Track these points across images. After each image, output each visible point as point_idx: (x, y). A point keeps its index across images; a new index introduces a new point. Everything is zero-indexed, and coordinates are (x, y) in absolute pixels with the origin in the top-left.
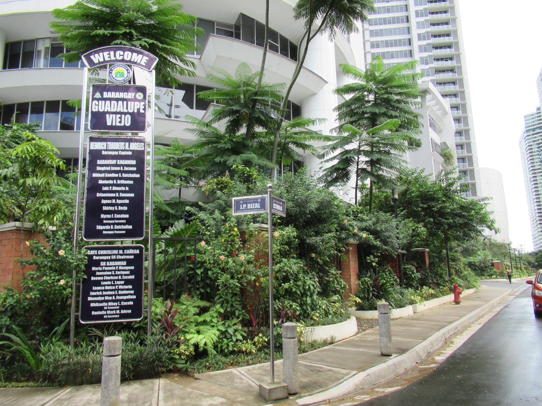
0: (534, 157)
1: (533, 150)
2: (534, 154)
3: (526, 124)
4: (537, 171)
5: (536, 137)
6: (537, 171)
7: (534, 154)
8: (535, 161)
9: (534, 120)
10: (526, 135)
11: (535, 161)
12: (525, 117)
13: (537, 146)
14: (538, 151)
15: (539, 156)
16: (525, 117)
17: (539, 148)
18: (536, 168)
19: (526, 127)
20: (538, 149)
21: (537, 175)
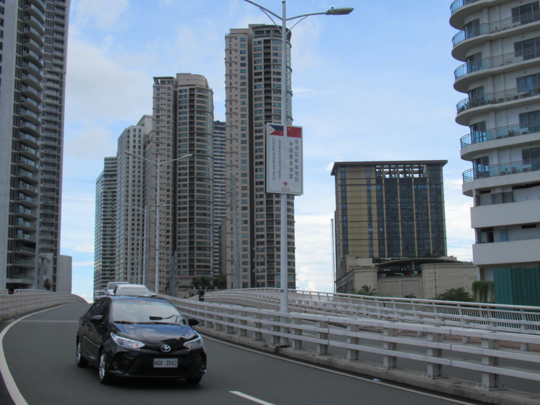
0: (108, 206)
1: (108, 198)
2: (108, 202)
3: (105, 167)
4: (108, 221)
5: (112, 184)
6: (108, 221)
7: (108, 202)
8: (108, 210)
9: (113, 161)
10: (103, 179)
11: (108, 210)
12: (106, 159)
13: (111, 194)
14: (111, 200)
15: (111, 206)
16: (106, 159)
17: (113, 196)
18: (107, 217)
19: (106, 171)
20: (111, 198)
21: (107, 225)
